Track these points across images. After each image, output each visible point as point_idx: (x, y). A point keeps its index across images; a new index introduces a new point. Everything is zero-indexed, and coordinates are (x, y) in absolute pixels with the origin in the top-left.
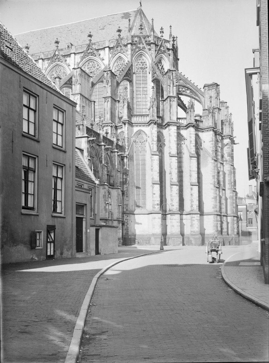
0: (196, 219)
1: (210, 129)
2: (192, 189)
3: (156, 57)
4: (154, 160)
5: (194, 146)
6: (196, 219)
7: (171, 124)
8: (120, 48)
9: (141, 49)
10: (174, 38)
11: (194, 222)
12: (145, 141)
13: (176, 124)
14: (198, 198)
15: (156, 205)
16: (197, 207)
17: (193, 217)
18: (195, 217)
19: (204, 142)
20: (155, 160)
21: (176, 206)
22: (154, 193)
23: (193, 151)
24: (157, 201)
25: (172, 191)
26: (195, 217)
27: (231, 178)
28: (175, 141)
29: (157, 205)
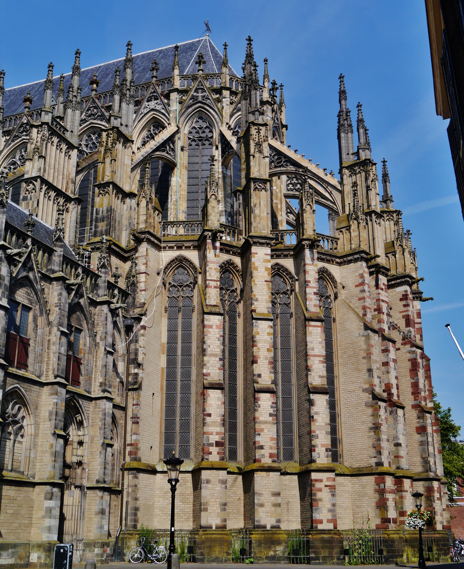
0: (326, 486)
1: (356, 256)
2: (311, 403)
3: (231, 116)
4: (211, 327)
5: (315, 294)
6: (326, 486)
7: (256, 240)
8: (156, 102)
9: (200, 99)
10: (274, 83)
11: (319, 495)
12: (191, 283)
13: (268, 241)
14: (329, 429)
15: (211, 445)
16: (327, 450)
17: (316, 480)
18: (321, 481)
19: (343, 287)
20: (214, 327)
21: (271, 448)
22: (207, 412)
23: (315, 306)
24: (217, 433)
25: (259, 407)
26: (321, 481)
27: (418, 379)
28: (266, 281)
29: (216, 446)
